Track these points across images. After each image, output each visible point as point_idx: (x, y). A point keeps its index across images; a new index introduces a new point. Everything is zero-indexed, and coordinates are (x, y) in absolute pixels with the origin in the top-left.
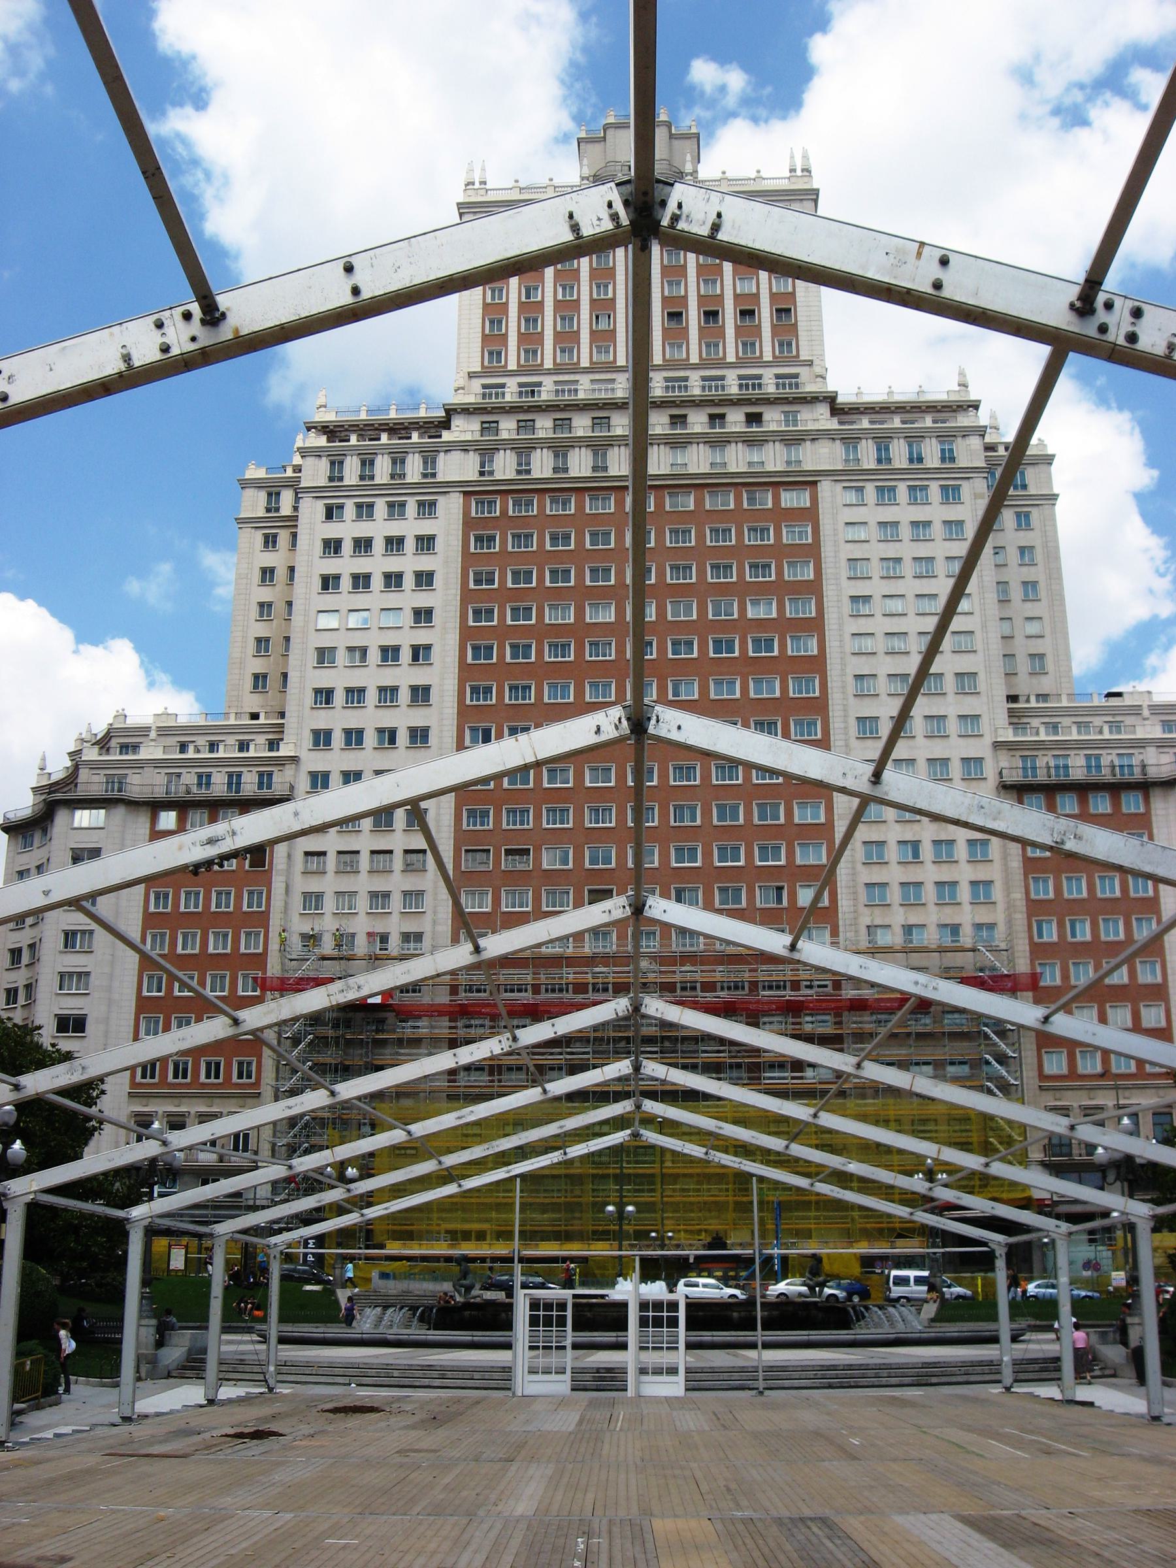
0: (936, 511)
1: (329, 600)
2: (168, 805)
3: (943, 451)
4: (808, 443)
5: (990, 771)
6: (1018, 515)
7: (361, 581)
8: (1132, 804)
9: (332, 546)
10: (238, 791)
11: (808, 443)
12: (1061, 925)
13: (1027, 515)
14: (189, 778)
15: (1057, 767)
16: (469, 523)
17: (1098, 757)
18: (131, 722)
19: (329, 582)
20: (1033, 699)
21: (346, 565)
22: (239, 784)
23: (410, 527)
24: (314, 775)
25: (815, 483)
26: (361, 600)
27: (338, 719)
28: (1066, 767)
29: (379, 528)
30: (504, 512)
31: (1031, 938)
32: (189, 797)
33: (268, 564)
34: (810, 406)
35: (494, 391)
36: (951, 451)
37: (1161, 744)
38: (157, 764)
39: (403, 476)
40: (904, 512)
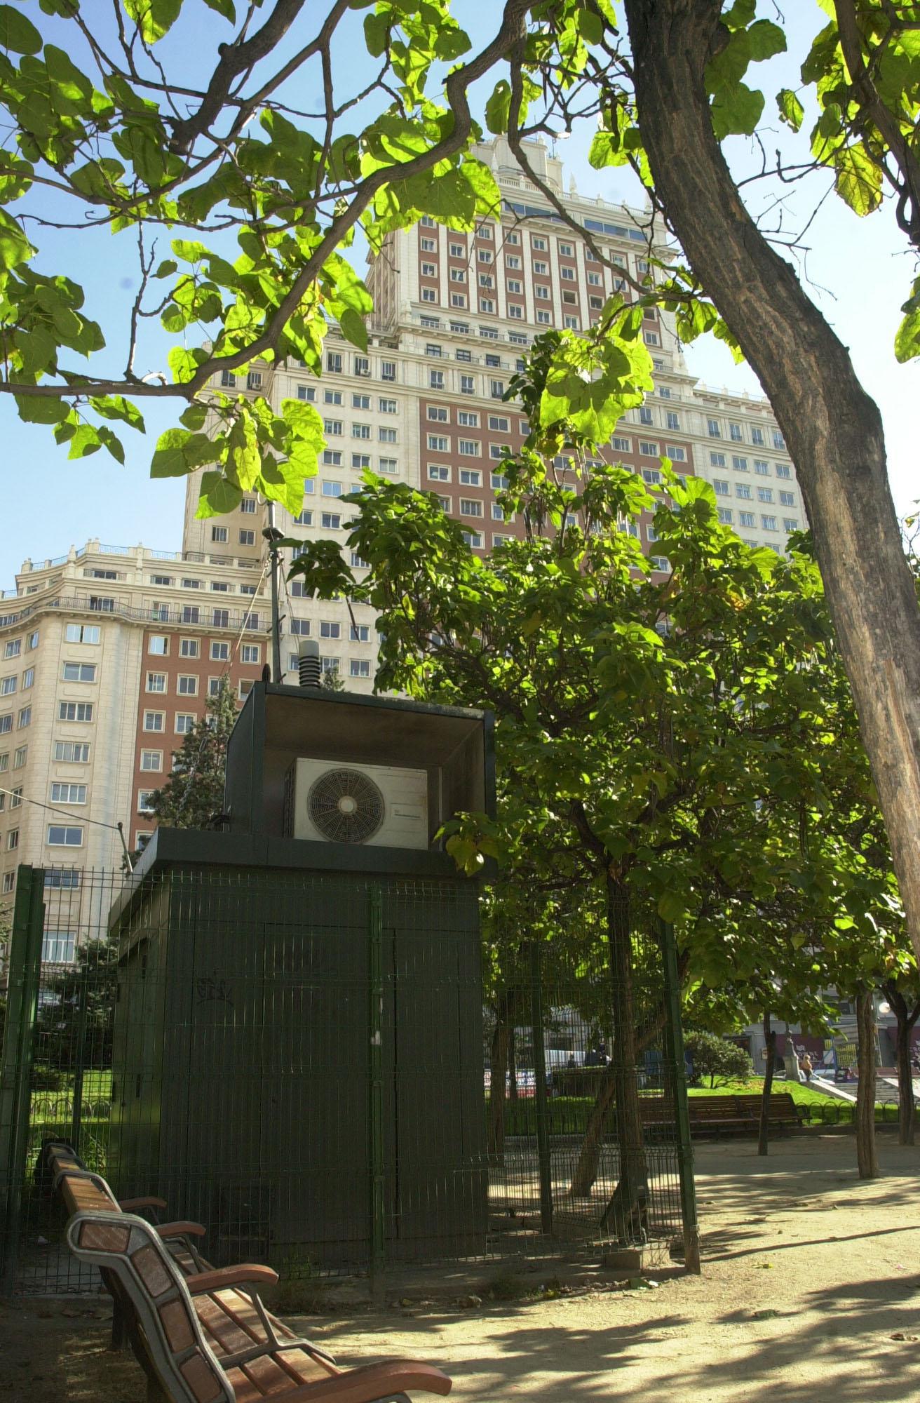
2: (161, 631)
14: (176, 608)
16: (425, 427)
23: (374, 418)
25: (689, 446)
30: (454, 420)
34: (677, 385)
38: (144, 591)
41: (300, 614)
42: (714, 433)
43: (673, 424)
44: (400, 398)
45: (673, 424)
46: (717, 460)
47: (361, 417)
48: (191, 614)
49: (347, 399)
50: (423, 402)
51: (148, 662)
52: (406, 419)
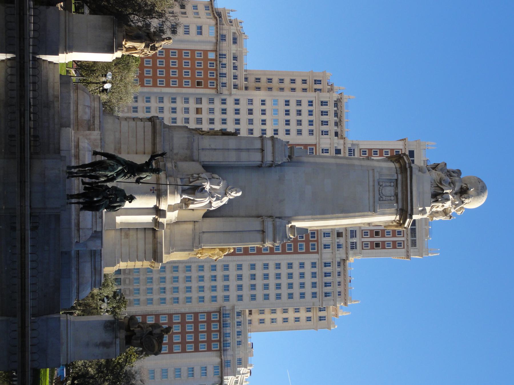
0: (308, 290)
1: (282, 103)
2: (216, 56)
3: (329, 293)
4: (331, 251)
5: (226, 304)
6: (310, 318)
7: (287, 112)
8: (215, 346)
9: (299, 103)
10: (220, 77)
11: (331, 251)
12: (178, 323)
13: (310, 320)
14: (224, 61)
15: (226, 324)
16: (306, 146)
17: (229, 336)
18: (244, 41)
19: (287, 103)
20: (249, 318)
21: (293, 108)
22: (223, 77)
23: (305, 127)
24: (225, 100)
25: (317, 253)
26: (282, 113)
27: (243, 107)
28: (226, 327)
29: (305, 118)
31: (174, 314)
32: (218, 62)
33: (297, 81)
35: (353, 153)
36: (329, 296)
37: (233, 356)
39: (322, 125)
40: (308, 280)
41: (228, 101)
42: (326, 265)
43: (326, 246)
44: (315, 137)
45: (326, 246)
46: (314, 265)
47: (305, 123)
48: (224, 66)
49: (311, 118)
50: (315, 145)
51: (206, 52)
52: (305, 139)
